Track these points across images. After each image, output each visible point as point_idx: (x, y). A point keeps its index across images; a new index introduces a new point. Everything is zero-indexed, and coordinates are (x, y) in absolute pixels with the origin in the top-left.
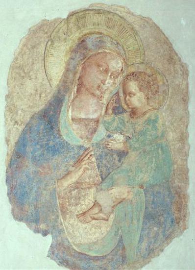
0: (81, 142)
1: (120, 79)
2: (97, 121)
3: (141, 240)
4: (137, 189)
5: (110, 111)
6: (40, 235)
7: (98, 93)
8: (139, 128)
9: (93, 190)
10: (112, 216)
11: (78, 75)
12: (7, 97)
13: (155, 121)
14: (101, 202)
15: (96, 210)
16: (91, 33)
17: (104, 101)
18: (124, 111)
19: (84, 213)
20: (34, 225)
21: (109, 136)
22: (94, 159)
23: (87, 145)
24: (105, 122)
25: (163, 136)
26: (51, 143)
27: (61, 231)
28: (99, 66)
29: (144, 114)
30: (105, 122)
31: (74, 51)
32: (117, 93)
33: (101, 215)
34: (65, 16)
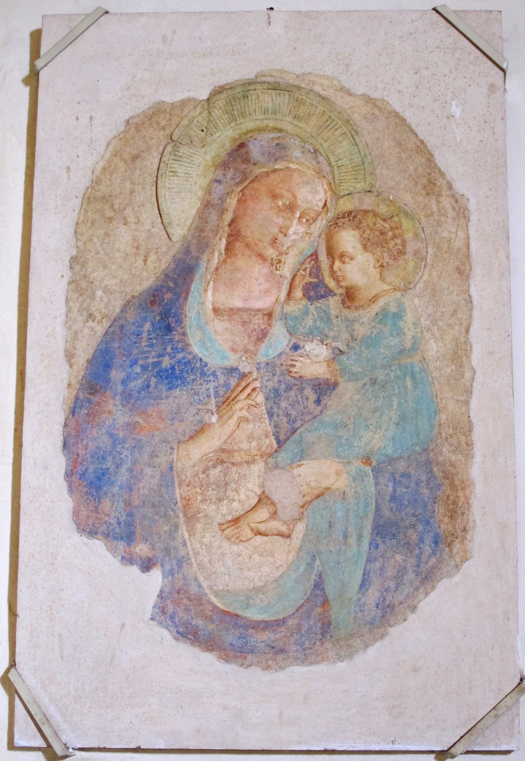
0: (232, 360)
1: (321, 223)
2: (270, 315)
3: (364, 584)
4: (357, 465)
5: (298, 293)
6: (135, 570)
7: (271, 253)
8: (361, 331)
9: (258, 467)
10: (300, 528)
11: (228, 217)
12: (74, 260)
13: (398, 316)
14: (276, 497)
15: (263, 513)
16: (260, 130)
17: (287, 271)
18: (329, 292)
19: (236, 521)
20: (121, 545)
21: (296, 348)
22: (260, 398)
23: (245, 368)
24: (285, 317)
25: (415, 347)
26: (166, 362)
27: (182, 562)
28: (275, 197)
29: (374, 299)
30: (285, 317)
31: (224, 165)
32: (315, 256)
33: (276, 525)
34: (204, 96)
